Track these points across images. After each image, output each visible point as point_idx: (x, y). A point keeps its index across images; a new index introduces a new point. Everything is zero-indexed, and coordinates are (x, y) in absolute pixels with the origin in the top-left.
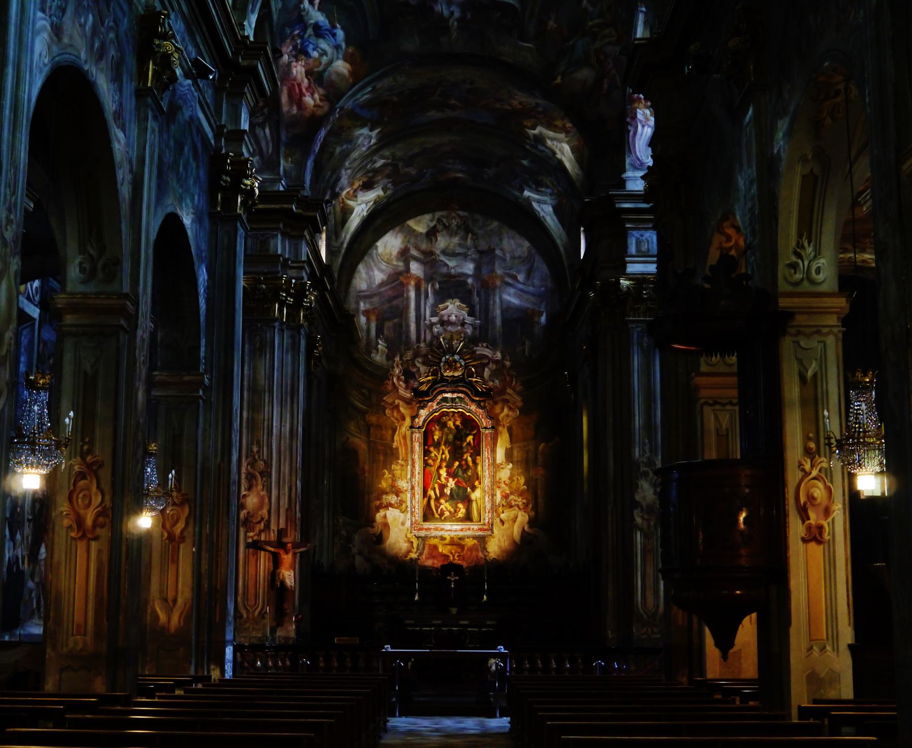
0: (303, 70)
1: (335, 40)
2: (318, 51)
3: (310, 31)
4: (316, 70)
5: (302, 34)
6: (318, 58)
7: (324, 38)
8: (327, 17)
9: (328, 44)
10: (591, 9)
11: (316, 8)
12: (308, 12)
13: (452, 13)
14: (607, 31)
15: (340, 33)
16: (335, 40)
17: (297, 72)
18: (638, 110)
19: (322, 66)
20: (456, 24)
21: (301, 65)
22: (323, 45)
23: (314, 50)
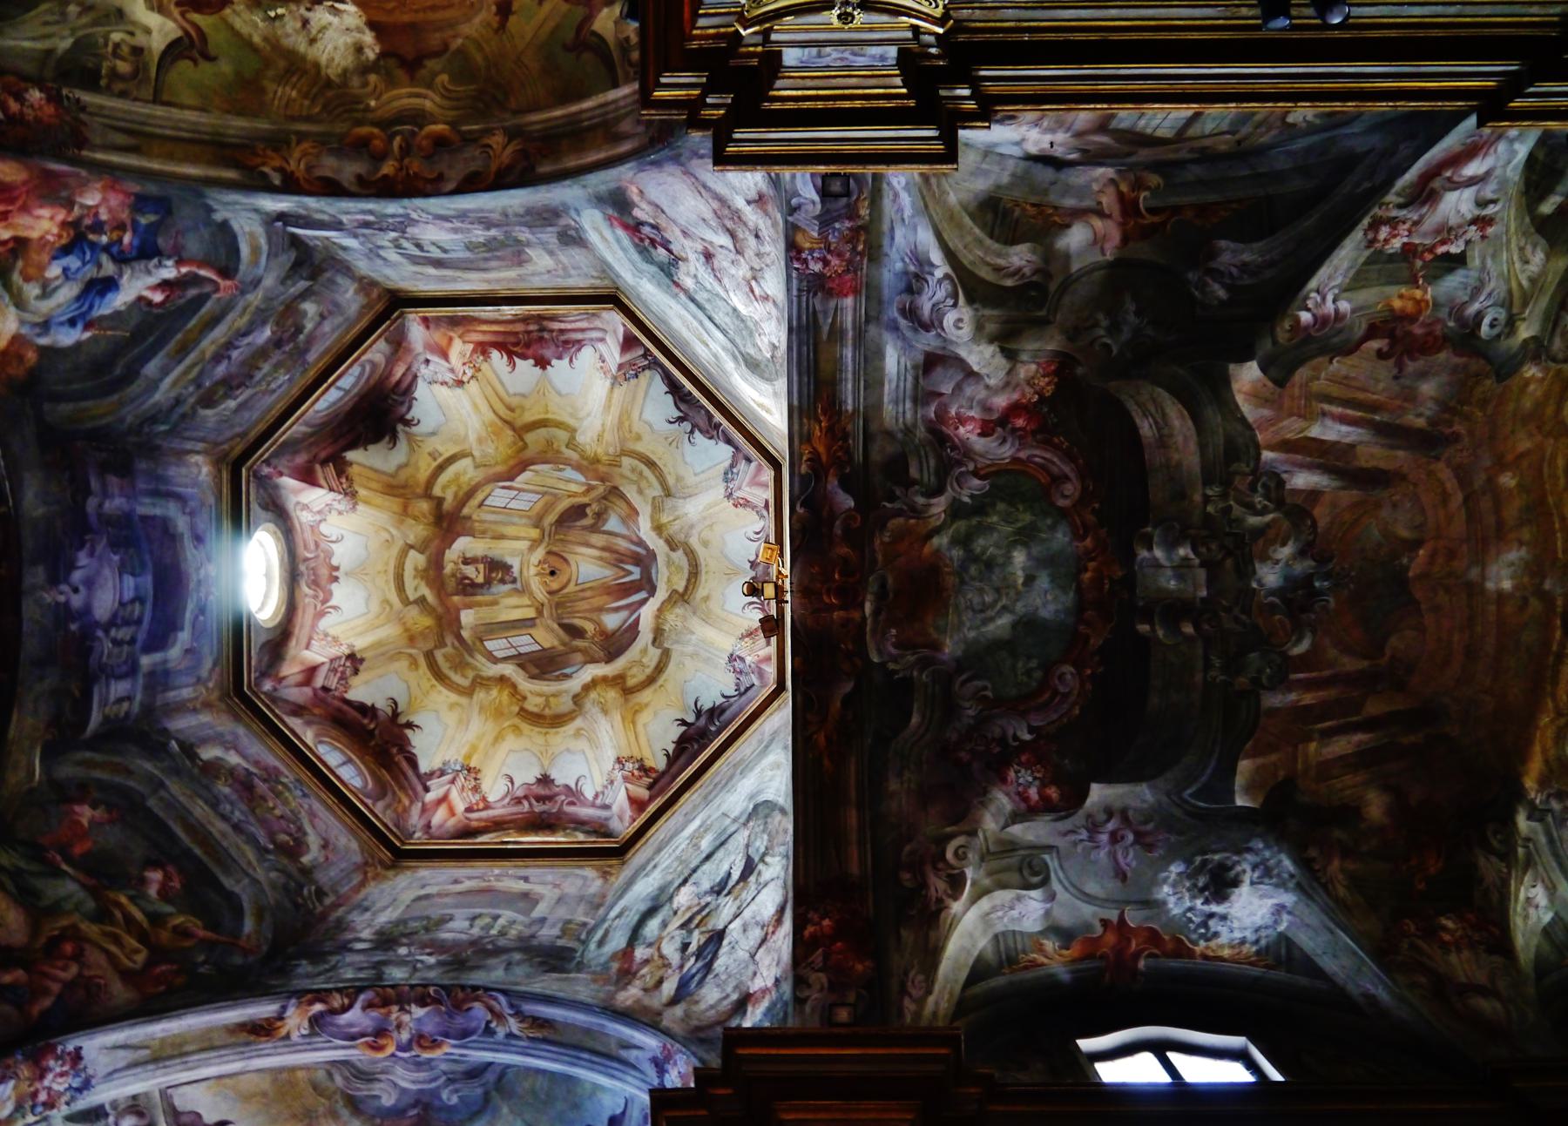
0: (35, 235)
1: (62, 324)
2: (57, 278)
3: (109, 268)
4: (20, 264)
5: (115, 250)
6: (43, 277)
7: (78, 298)
8: (117, 314)
9: (59, 306)
10: (153, 891)
11: (148, 294)
12: (149, 272)
13: (76, 590)
14: (133, 943)
15: (67, 338)
16: (62, 324)
17: (39, 217)
18: (12, 1083)
19: (20, 281)
20: (62, 599)
21: (47, 232)
22: (67, 293)
23: (65, 270)
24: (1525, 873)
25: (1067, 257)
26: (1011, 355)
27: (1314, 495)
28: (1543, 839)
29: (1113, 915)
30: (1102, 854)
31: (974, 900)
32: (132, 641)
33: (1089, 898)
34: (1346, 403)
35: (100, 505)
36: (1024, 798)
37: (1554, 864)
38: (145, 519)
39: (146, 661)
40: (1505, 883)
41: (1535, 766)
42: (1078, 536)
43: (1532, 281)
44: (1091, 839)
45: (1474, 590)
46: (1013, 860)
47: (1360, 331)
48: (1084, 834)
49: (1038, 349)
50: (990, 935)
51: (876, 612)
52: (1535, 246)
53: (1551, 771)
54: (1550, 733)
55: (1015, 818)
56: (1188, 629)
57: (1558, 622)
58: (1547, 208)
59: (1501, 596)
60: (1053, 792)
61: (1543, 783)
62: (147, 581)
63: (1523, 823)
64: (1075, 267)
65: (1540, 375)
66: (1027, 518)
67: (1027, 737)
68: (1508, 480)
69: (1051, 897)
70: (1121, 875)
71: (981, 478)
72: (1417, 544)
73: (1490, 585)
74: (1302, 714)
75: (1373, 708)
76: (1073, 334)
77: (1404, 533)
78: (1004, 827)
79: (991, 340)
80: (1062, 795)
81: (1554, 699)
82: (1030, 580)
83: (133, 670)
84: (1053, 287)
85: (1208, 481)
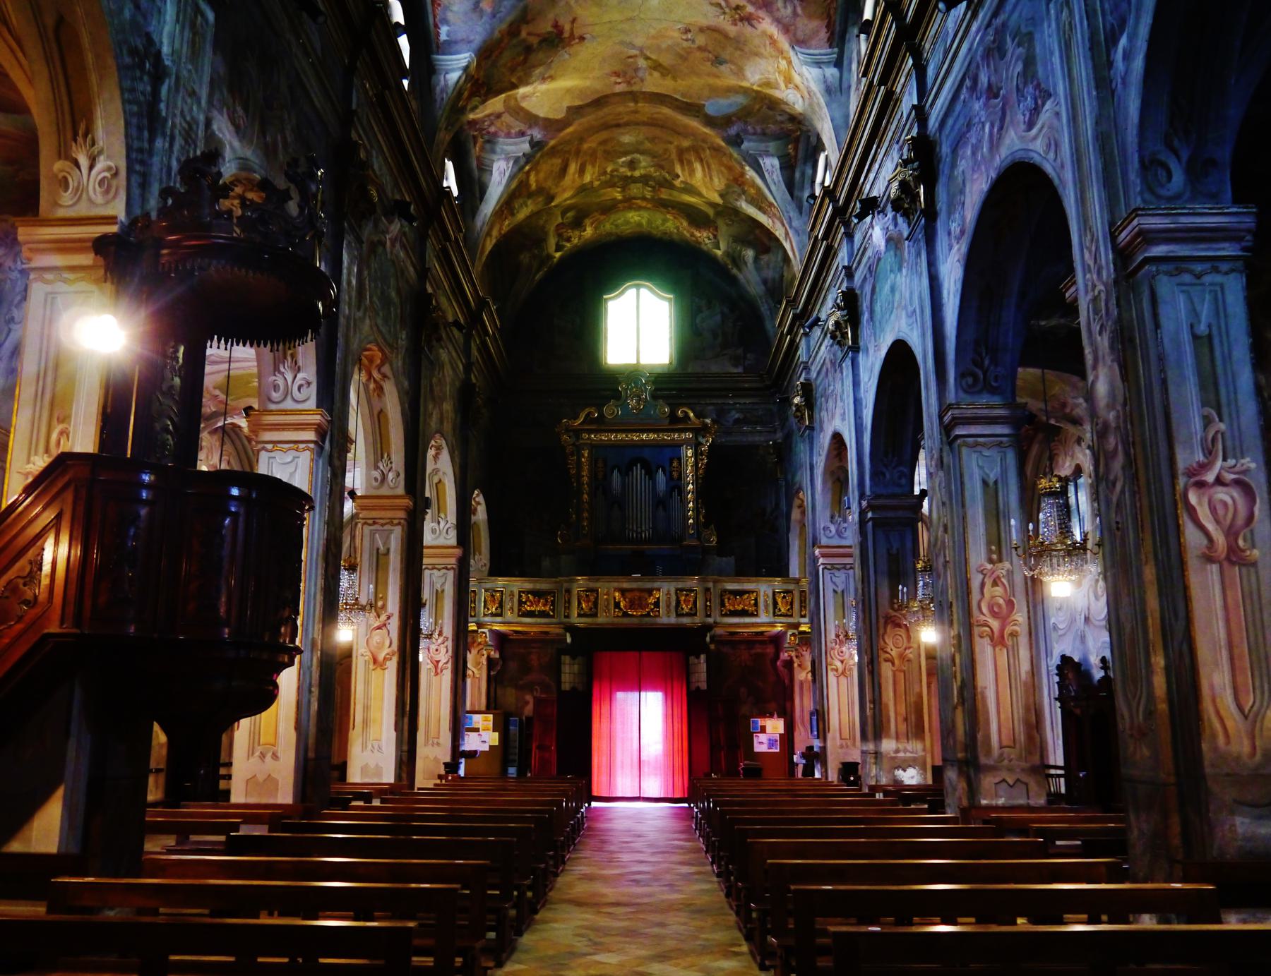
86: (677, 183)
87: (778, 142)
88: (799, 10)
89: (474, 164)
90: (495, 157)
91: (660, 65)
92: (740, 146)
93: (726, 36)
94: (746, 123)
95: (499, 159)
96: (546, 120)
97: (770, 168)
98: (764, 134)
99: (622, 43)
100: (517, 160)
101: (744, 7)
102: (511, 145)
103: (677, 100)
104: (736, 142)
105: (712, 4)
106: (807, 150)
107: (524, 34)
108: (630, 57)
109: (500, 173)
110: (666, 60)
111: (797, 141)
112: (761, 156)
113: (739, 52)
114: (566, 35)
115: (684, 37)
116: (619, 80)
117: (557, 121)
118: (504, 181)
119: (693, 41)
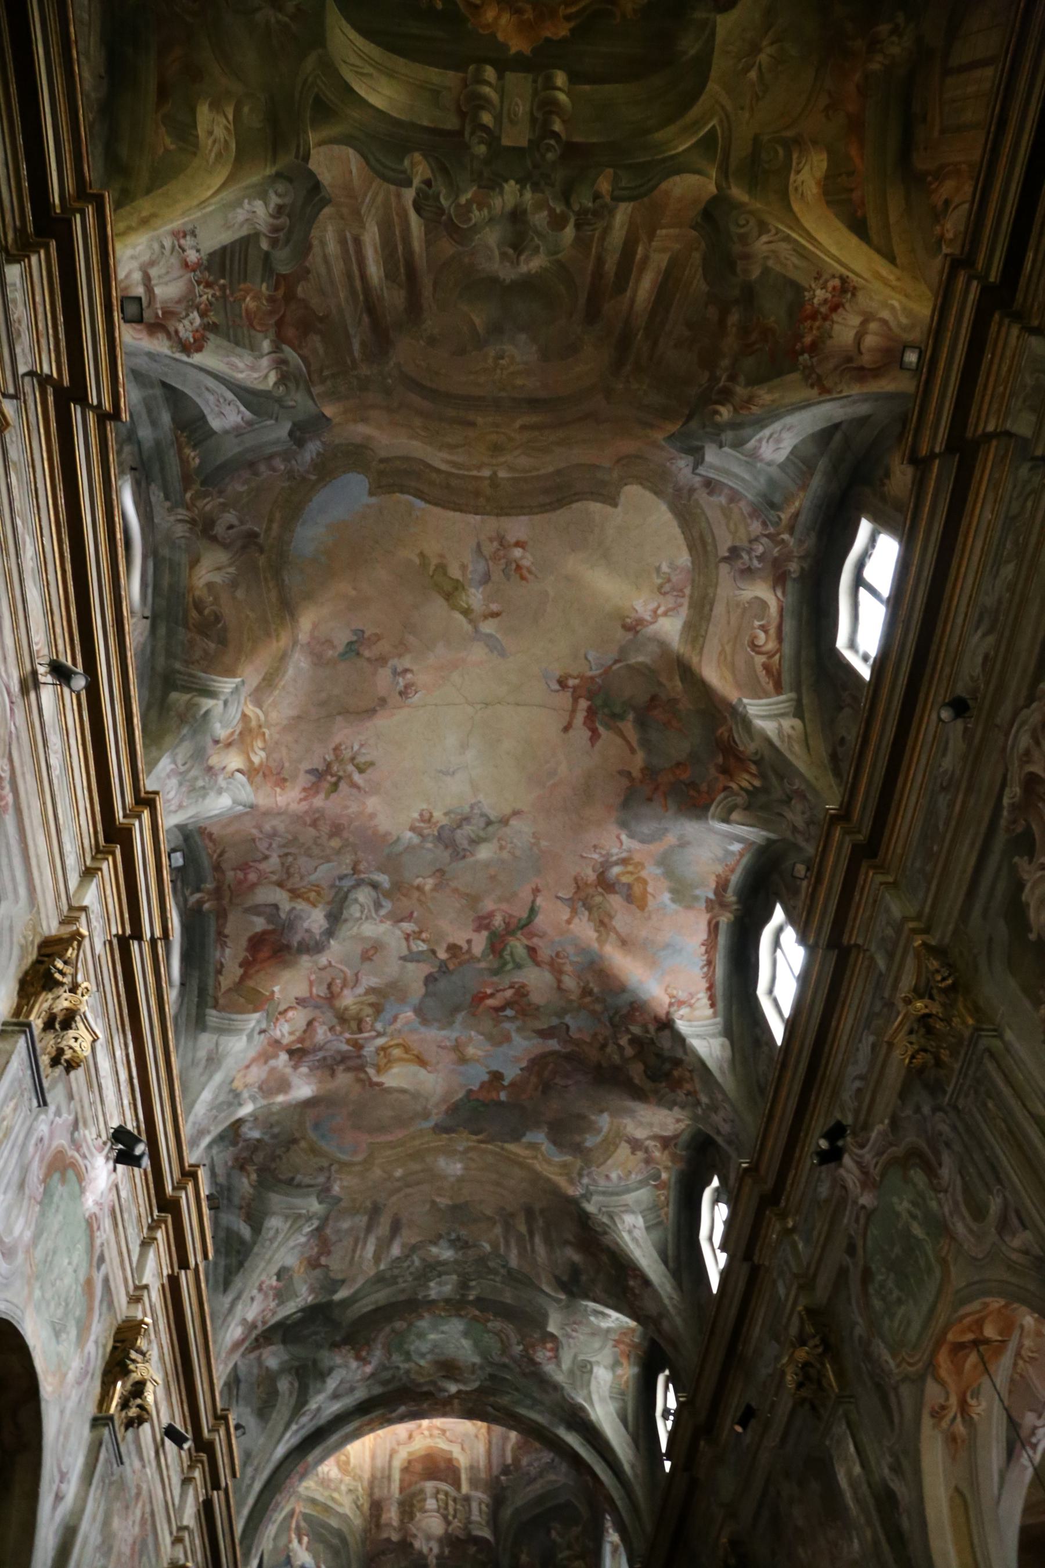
24: (615, 1224)
25: (281, 1363)
26: (331, 1370)
27: (403, 1246)
28: (601, 1198)
29: (611, 1343)
30: (582, 1337)
31: (592, 1404)
32: (455, 1500)
33: (601, 1348)
34: (354, 1251)
35: (395, 1529)
36: (550, 1359)
37: (615, 1198)
38: (402, 1490)
39: (465, 1488)
40: (617, 1244)
41: (562, 1182)
42: (421, 1317)
43: (287, 1217)
44: (573, 1338)
45: (460, 1180)
46: (578, 1373)
47: (318, 1272)
48: (571, 1341)
49: (328, 1358)
50: (609, 1401)
51: (457, 1381)
52: (269, 1229)
53: (567, 1174)
54: (545, 1166)
55: (559, 1365)
56: (473, 1283)
57: (483, 1146)
58: (246, 1231)
59: (466, 1169)
60: (549, 1345)
61: (571, 1182)
62: (429, 1486)
63: (590, 1208)
64: (286, 1357)
65: (338, 1182)
66: (413, 1337)
67: (521, 1347)
68: (399, 1173)
69: (598, 1363)
70: (593, 1334)
71: (391, 1355)
72: (433, 1203)
73: (459, 1173)
74: (522, 1254)
75: (523, 1229)
76: (319, 1346)
77: (428, 1206)
78: (561, 1370)
79: (324, 1382)
80: (551, 1342)
81: (525, 1158)
82: (443, 1332)
83: (467, 1499)
84: (296, 1364)
85: (397, 1283)
86: (420, 168)
87: (219, 462)
88: (255, 831)
89: (816, 482)
90: (774, 471)
91: (448, 596)
92: (294, 425)
93: (345, 712)
94: (290, 475)
95: (769, 464)
96: (658, 493)
97: (227, 410)
98: (252, 465)
99: (503, 654)
100: (738, 444)
101: (327, 797)
102: (736, 476)
103: (419, 495)
104: (300, 433)
105: (372, 764)
106: (162, 469)
107: (639, 759)
108: (495, 615)
109: (779, 441)
110: (439, 605)
111: (187, 480)
112: (249, 423)
113: (323, 695)
114: (583, 704)
115: (409, 676)
116: (518, 552)
117: (641, 481)
118: (777, 426)
119: (395, 673)
